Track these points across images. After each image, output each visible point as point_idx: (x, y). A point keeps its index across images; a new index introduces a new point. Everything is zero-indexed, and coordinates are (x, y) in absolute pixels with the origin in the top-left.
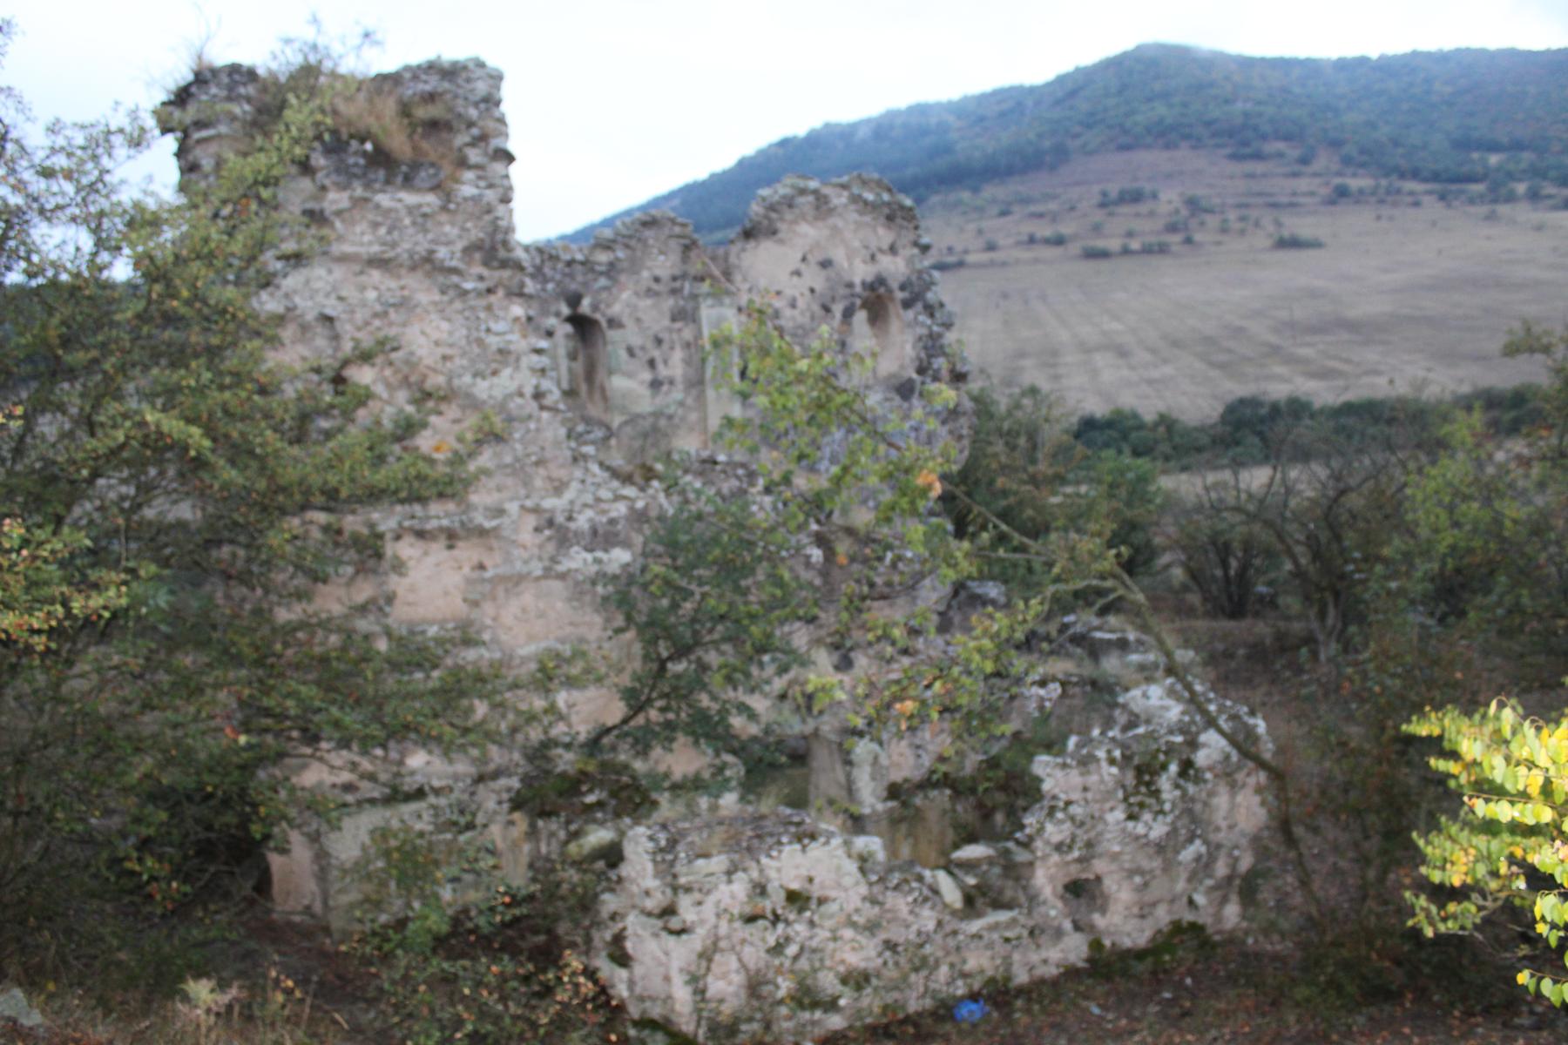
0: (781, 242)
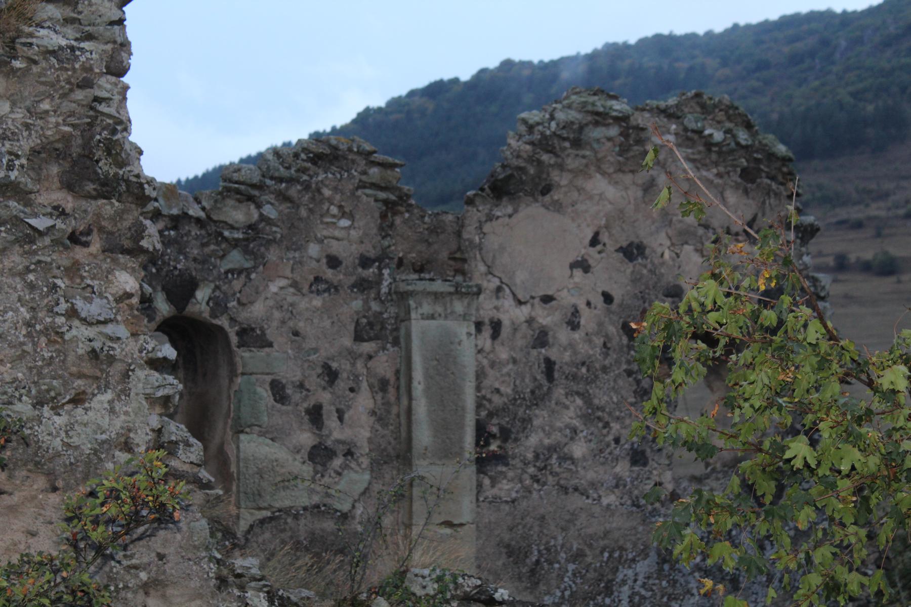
0: (558, 207)
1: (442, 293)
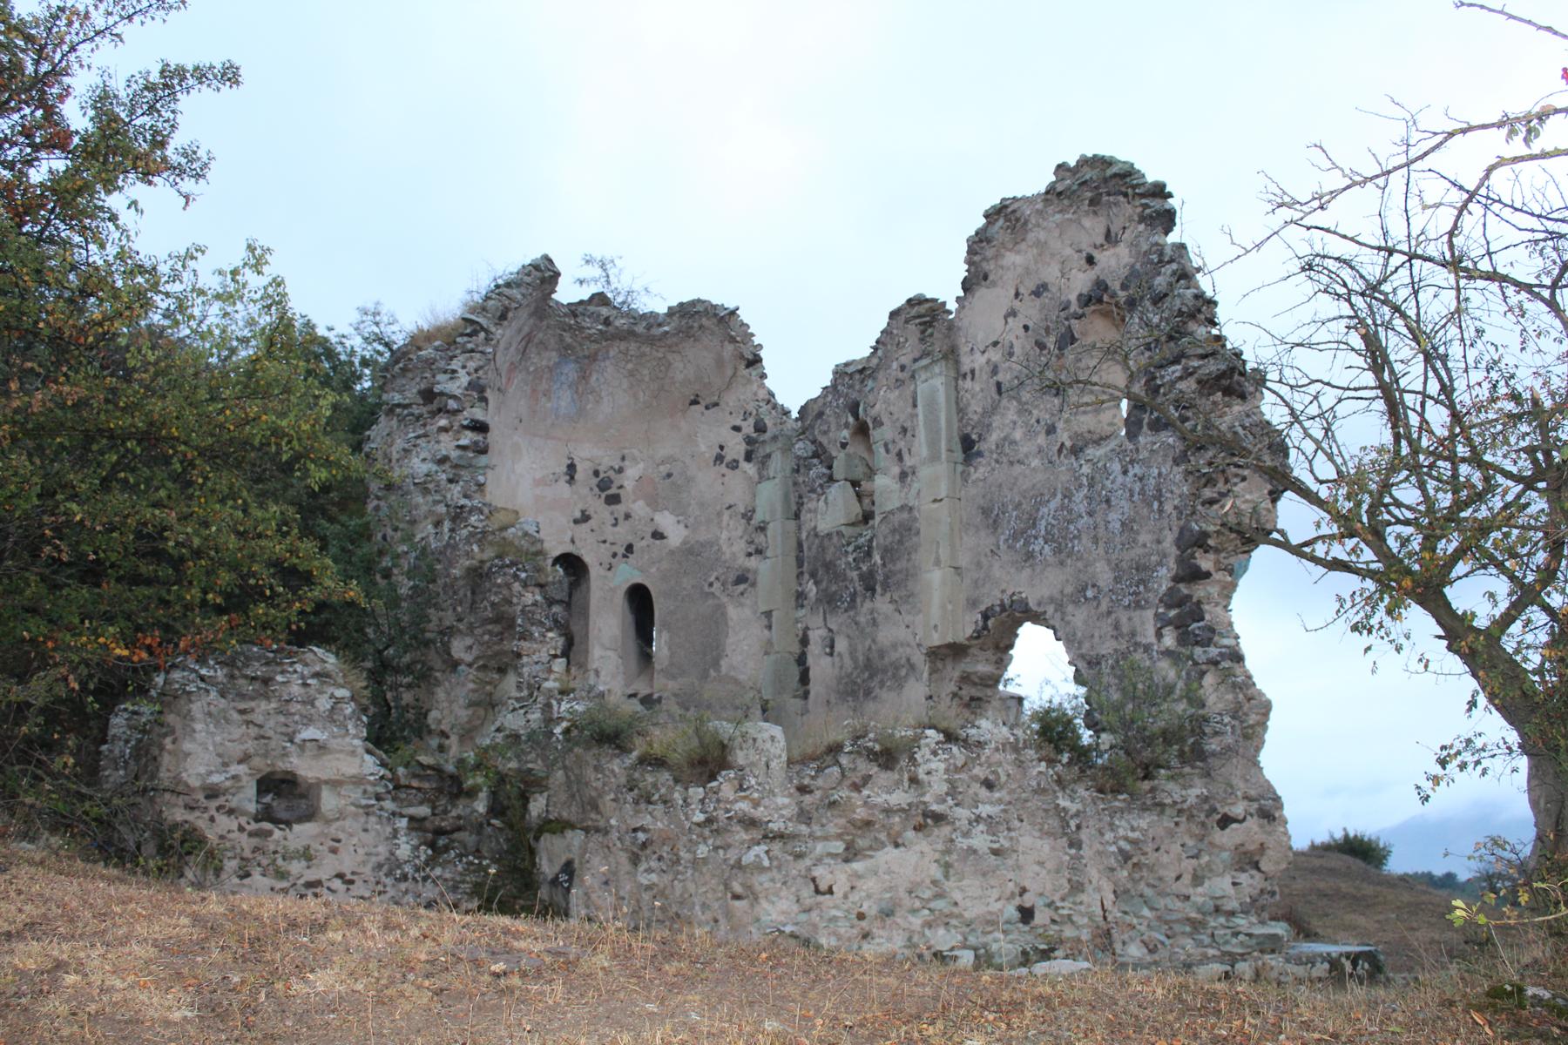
0: (994, 284)
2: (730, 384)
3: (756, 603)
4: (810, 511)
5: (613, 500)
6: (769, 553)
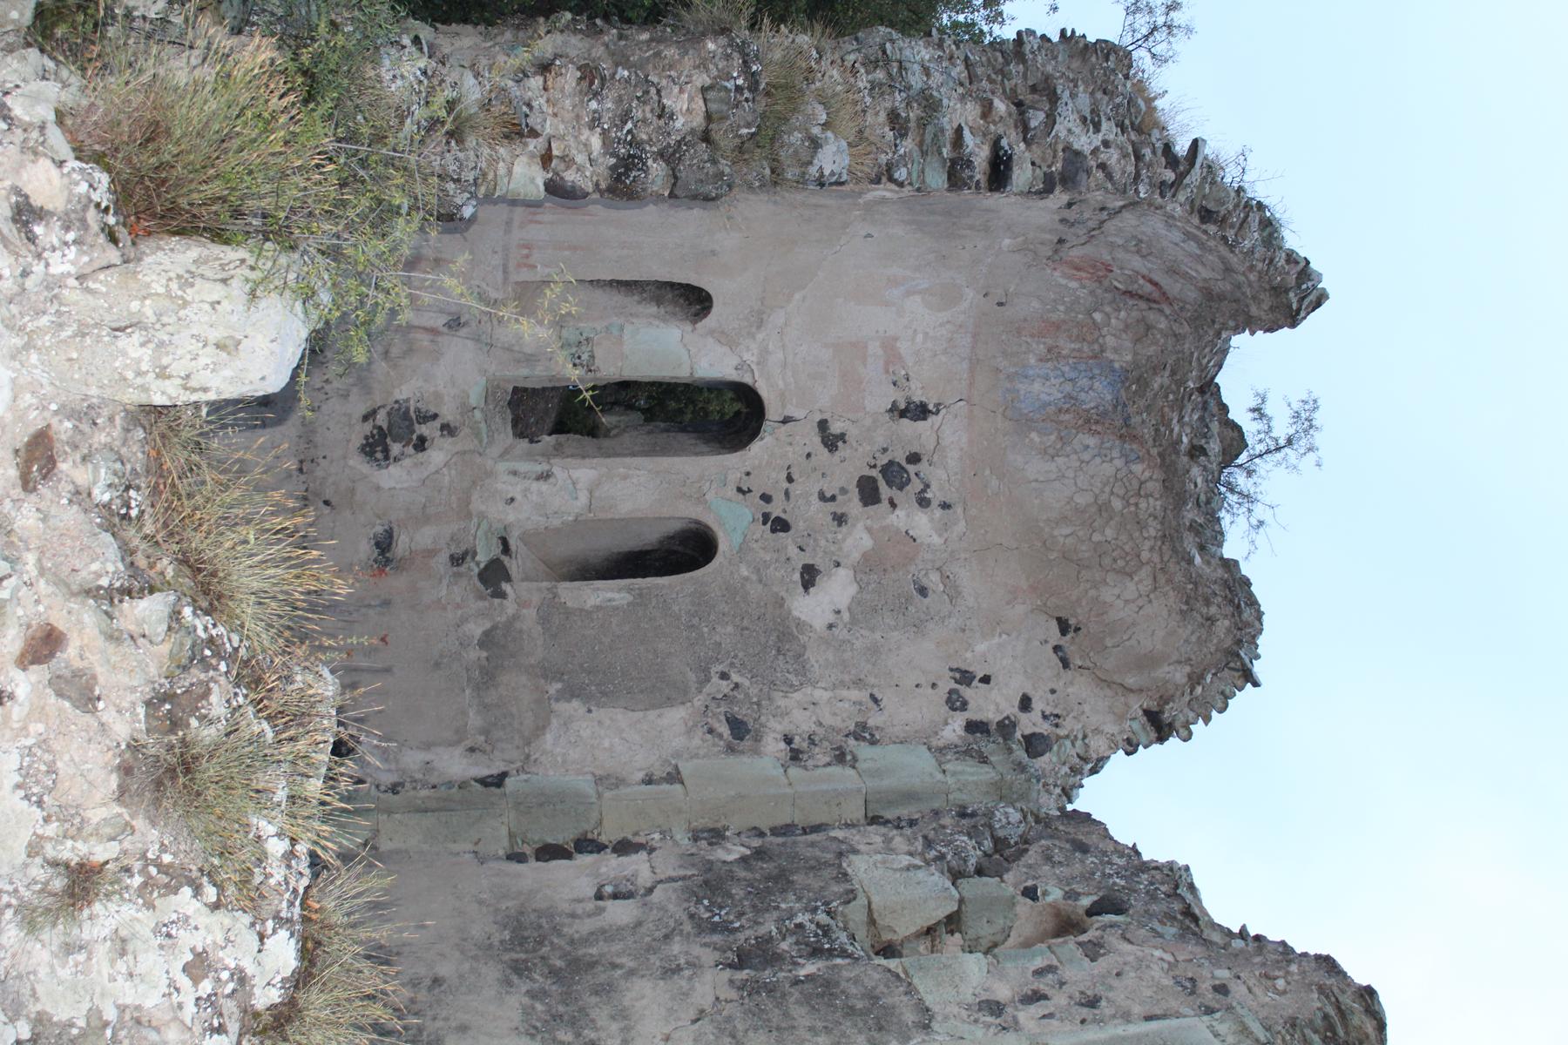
1: (1252, 1033)
2: (1110, 684)
3: (696, 756)
4: (888, 841)
5: (868, 492)
6: (794, 771)
